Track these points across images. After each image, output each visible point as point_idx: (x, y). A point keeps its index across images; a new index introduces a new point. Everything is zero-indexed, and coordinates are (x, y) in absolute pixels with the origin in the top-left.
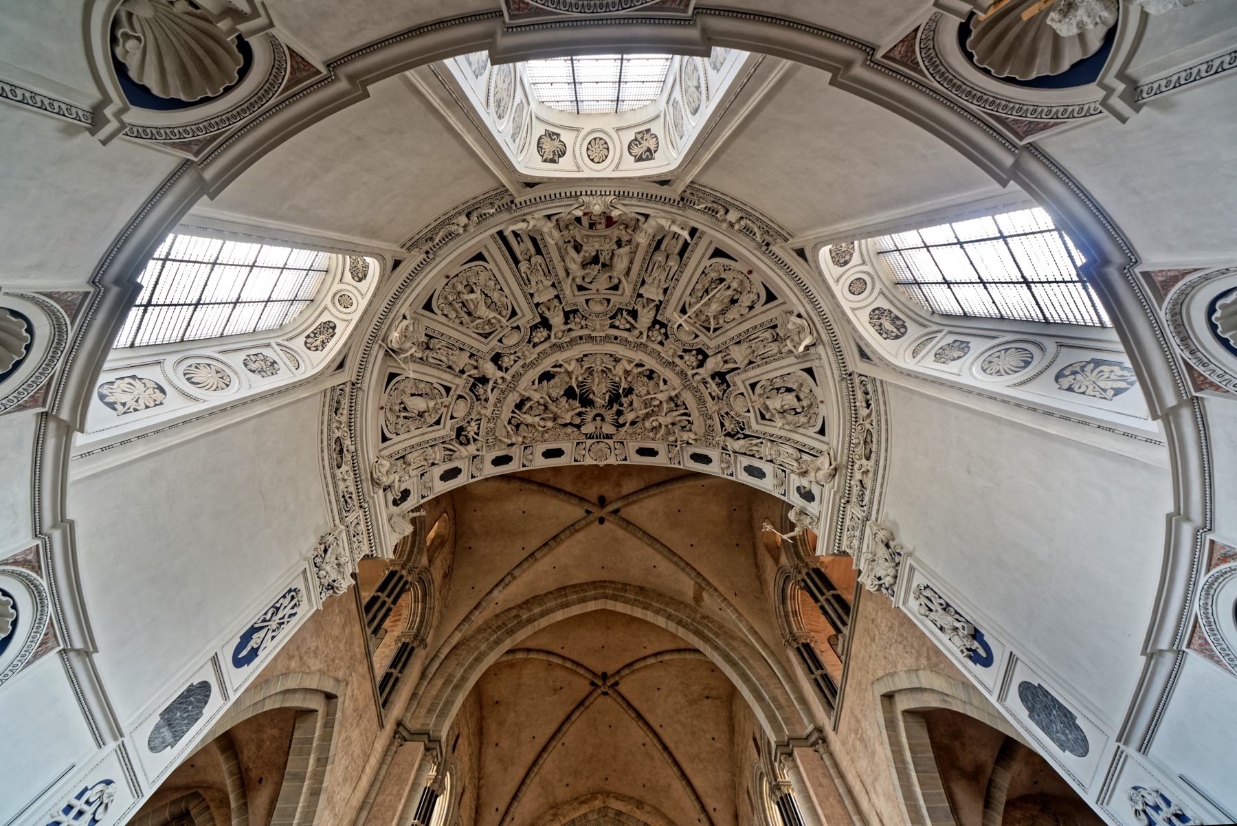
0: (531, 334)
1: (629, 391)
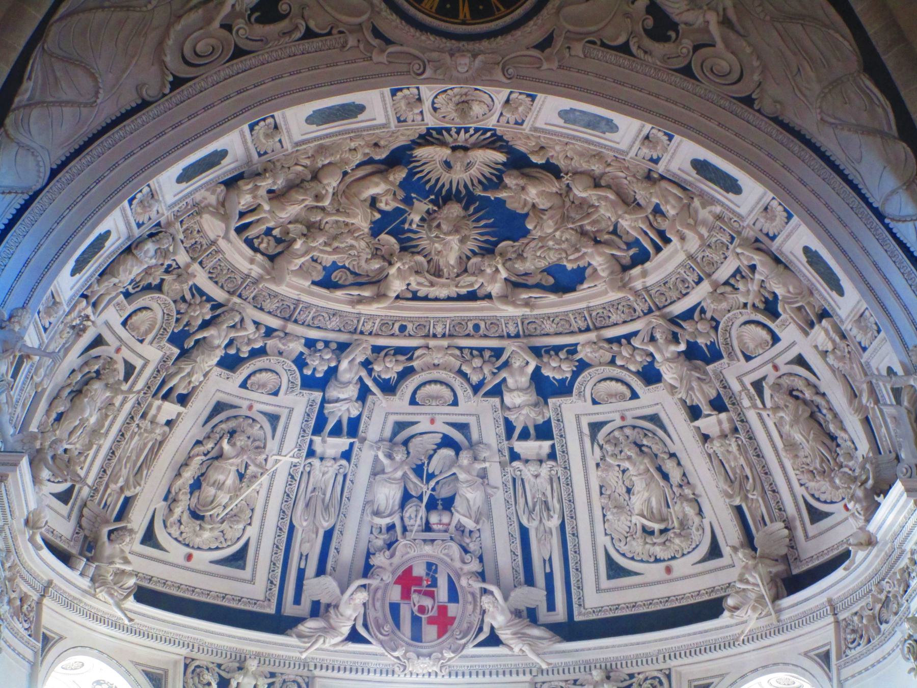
0: (576, 374)
1: (376, 230)
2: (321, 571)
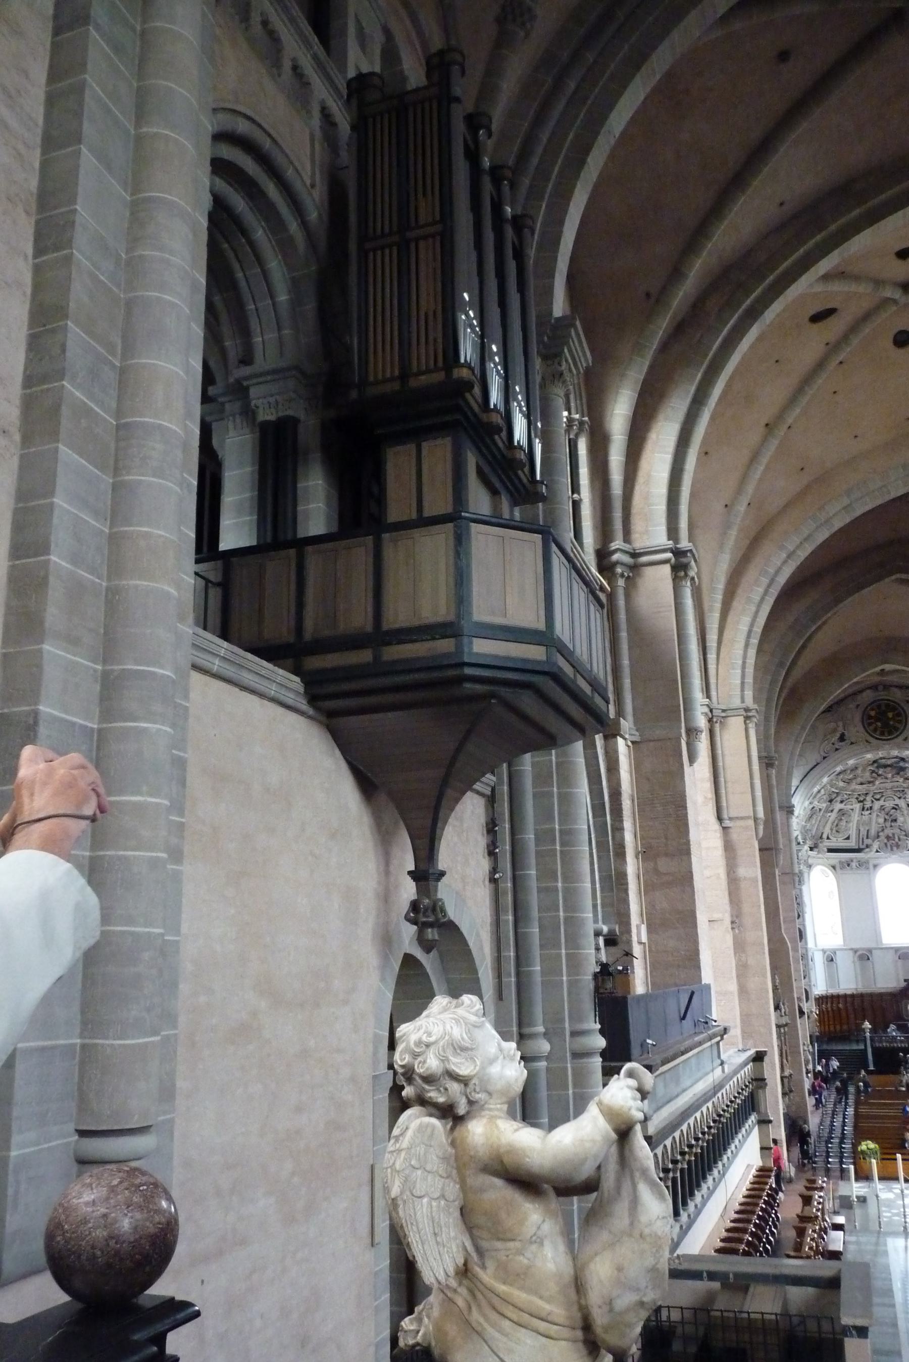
2: (867, 838)
